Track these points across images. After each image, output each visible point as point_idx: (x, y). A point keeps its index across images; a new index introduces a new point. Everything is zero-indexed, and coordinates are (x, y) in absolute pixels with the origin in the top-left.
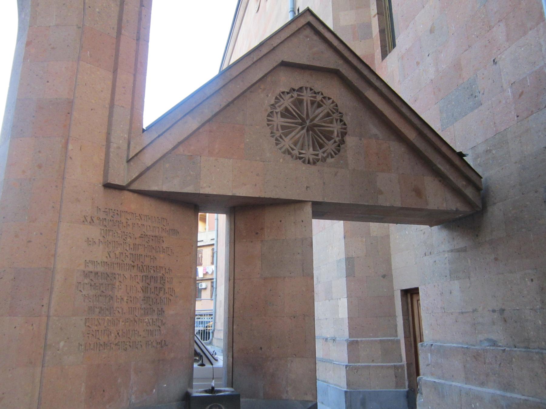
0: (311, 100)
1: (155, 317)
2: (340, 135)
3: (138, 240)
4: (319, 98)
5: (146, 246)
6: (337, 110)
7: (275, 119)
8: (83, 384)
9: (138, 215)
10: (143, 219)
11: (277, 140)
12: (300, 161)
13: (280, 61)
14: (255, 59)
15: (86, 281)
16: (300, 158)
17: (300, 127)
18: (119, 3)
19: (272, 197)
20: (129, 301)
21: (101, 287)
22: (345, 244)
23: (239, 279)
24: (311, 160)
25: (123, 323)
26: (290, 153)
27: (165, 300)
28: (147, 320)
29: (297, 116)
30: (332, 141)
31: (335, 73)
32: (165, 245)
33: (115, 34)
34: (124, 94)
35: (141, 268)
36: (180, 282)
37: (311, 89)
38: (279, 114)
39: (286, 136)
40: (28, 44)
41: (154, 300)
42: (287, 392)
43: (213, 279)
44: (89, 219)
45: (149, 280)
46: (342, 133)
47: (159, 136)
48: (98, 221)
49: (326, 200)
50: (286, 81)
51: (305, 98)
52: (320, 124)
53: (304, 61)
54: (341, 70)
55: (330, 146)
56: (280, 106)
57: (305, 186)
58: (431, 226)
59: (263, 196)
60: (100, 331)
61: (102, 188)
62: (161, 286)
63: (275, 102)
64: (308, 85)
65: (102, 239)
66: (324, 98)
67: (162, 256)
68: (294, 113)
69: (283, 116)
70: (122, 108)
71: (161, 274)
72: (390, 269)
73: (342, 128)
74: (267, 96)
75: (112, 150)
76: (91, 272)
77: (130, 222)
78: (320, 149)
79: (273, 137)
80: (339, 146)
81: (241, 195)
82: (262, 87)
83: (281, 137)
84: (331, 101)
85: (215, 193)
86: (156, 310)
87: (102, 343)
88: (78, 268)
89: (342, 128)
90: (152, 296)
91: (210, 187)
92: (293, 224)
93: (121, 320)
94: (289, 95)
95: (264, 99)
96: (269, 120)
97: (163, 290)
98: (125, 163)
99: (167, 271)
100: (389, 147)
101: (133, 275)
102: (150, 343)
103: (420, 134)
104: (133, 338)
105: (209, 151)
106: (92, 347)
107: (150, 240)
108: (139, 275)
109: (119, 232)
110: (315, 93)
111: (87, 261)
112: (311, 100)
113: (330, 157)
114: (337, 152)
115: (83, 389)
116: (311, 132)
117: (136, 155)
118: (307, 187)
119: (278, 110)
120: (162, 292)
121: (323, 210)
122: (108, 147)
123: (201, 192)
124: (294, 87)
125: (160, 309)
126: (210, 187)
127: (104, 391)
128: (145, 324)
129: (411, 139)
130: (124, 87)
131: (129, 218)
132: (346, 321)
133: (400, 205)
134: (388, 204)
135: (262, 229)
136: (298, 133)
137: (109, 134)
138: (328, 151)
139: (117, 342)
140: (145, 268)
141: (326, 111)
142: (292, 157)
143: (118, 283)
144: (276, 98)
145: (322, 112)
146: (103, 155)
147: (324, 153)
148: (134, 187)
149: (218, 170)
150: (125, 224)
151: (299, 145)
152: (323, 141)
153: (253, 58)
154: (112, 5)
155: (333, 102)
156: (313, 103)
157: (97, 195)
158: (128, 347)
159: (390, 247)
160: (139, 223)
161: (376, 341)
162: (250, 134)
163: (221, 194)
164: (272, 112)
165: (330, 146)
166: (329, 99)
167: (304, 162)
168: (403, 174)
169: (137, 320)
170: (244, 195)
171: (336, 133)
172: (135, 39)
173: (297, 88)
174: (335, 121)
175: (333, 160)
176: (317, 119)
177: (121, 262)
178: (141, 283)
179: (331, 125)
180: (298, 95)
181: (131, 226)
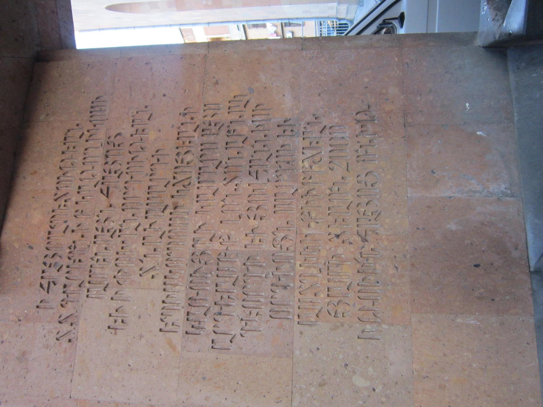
1: (299, 142)
5: (128, 178)
8: (459, 320)
9: (57, 204)
10: (63, 190)
15: (209, 325)
20: (260, 213)
25: (313, 224)
27: (256, 118)
28: (306, 164)
32: (127, 130)
35: (179, 187)
41: (258, 146)
44: (65, 328)
45: (210, 163)
62: (223, 132)
65: (110, 292)
67: (151, 135)
76: (188, 313)
86: (281, 141)
87: (359, 278)
88: (179, 348)
90: (247, 153)
93: (306, 231)
99: (188, 119)
101: (196, 206)
102: (361, 152)
104: (350, 198)
106: (368, 304)
107: (114, 168)
108: (196, 192)
111: (162, 325)
115: (472, 321)
120: (238, 128)
125: (280, 131)
127: (477, 266)
128: (315, 168)
131: (64, 226)
139: (358, 239)
140: (179, 177)
143: (216, 245)
150: (76, 236)
157: (11, 311)
160: (74, 199)
169: (307, 188)
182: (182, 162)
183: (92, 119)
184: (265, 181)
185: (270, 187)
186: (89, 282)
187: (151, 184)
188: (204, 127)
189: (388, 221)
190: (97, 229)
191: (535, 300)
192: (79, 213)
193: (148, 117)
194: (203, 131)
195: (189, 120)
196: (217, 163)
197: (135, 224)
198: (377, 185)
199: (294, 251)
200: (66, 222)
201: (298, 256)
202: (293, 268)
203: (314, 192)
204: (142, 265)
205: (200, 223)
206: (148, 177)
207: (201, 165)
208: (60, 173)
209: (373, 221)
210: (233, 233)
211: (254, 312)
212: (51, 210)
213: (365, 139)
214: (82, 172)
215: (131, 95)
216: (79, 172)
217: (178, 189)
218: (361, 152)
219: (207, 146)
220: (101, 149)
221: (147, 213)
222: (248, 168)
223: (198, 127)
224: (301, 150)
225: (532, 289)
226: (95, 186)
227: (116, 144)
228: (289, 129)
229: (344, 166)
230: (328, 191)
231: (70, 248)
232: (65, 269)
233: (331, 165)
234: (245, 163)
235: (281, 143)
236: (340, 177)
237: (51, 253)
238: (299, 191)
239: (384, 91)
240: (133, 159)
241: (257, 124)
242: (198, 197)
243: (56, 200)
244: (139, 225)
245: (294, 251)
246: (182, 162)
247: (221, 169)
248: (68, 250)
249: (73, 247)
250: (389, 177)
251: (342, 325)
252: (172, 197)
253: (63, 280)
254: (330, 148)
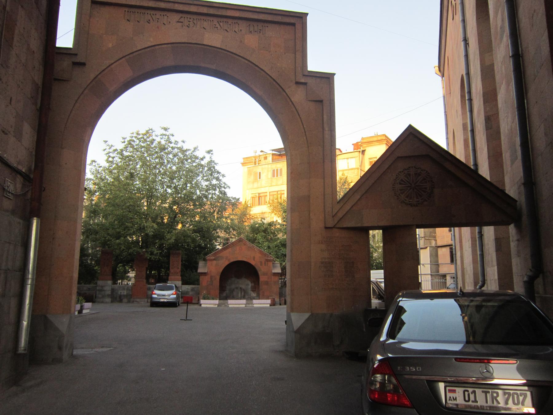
31: (427, 156)
40: (291, 173)
43: (452, 245)
69: (400, 184)
137: (324, 206)
148: (337, 226)
156: (416, 174)
167: (411, 206)
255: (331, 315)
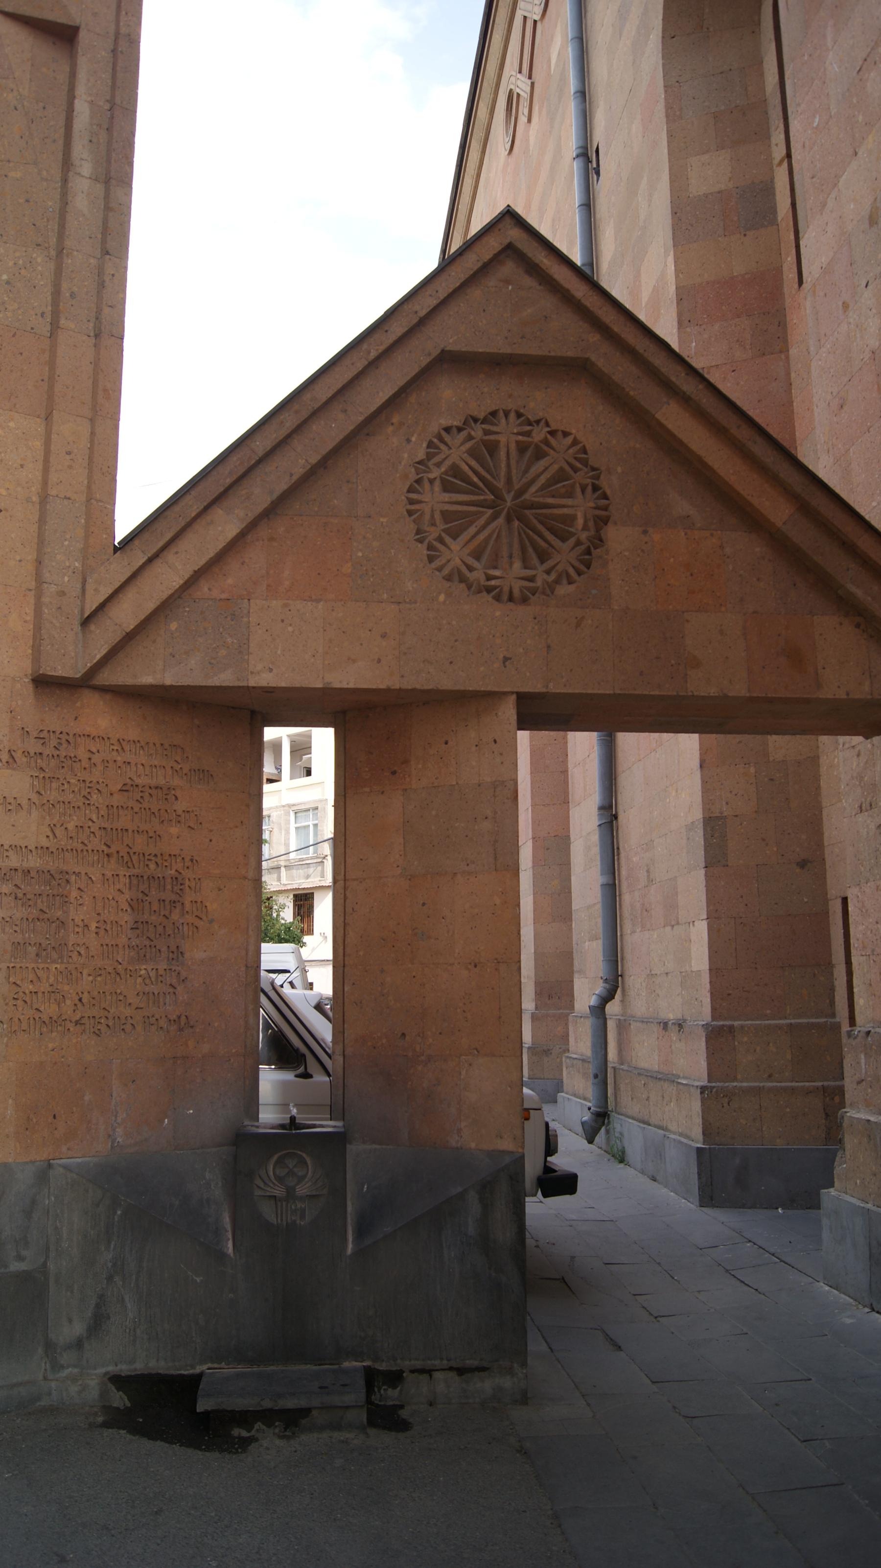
0: (517, 442)
2: (591, 524)
3: (116, 796)
4: (539, 434)
5: (136, 809)
6: (585, 462)
7: (426, 497)
8: (10, 1101)
10: (127, 748)
11: (430, 547)
12: (488, 598)
13: (435, 353)
14: (373, 354)
16: (489, 590)
17: (490, 512)
18: (53, 253)
19: (418, 687)
20: (102, 932)
21: (39, 901)
22: (704, 782)
23: (356, 880)
24: (516, 593)
25: (91, 978)
26: (462, 579)
28: (143, 972)
29: (481, 485)
30: (572, 541)
31: (577, 369)
33: (49, 328)
34: (70, 467)
35: (126, 858)
36: (220, 890)
37: (519, 415)
38: (437, 483)
39: (455, 537)
41: (160, 929)
42: (459, 1131)
46: (597, 518)
47: (150, 560)
48: (25, 760)
49: (553, 688)
50: (453, 399)
51: (503, 439)
52: (541, 500)
53: (499, 346)
54: (593, 358)
55: (565, 555)
56: (438, 465)
57: (501, 657)
58: (867, 738)
59: (397, 687)
60: (40, 995)
61: (31, 687)
62: (174, 897)
63: (427, 454)
64: (511, 405)
65: (35, 797)
66: (552, 433)
67: (174, 830)
68: (475, 479)
69: (447, 487)
70: (66, 502)
71: (173, 872)
72: (820, 845)
73: (597, 508)
74: (408, 441)
75: (46, 600)
76: (16, 870)
77: (96, 758)
78: (542, 562)
79: (420, 541)
80: (588, 552)
81: (344, 685)
82: (395, 420)
83: (440, 540)
84: (569, 440)
85: (283, 685)
86: (164, 949)
87: (45, 1018)
89: (597, 508)
90: (154, 918)
91: (271, 670)
92: (474, 749)
93: (85, 972)
94: (464, 434)
95: (399, 449)
96: (411, 502)
97: (178, 905)
98: (77, 628)
100: (721, 547)
101: (109, 874)
103: (804, 508)
104: (112, 1010)
105: (268, 586)
107: (146, 795)
108: (121, 873)
109: (73, 781)
110: (530, 424)
112: (517, 442)
113: (565, 581)
114: (582, 568)
116: (516, 523)
117: (102, 606)
118: (506, 659)
119: (435, 473)
120: (177, 911)
121: (543, 713)
122: (39, 595)
123: (252, 683)
124: (475, 413)
125: (173, 948)
126: (271, 670)
127: (54, 1117)
128: (139, 980)
129: (779, 524)
130: (68, 453)
131: (94, 750)
132: (706, 978)
133: (744, 693)
134: (713, 691)
135: (406, 762)
136: (484, 527)
138: (560, 568)
139: (78, 1017)
140: (135, 858)
141: (556, 467)
142: (469, 587)
143: (74, 893)
144: (430, 445)
145: (546, 469)
146: (29, 610)
147: (548, 572)
149: (290, 629)
150: (85, 763)
151: (485, 558)
152: (546, 541)
153: (369, 352)
154: (39, 260)
155: (575, 442)
156: (522, 448)
157: (20, 702)
158: (103, 1028)
159: (818, 788)
160: (119, 758)
161: (779, 1027)
162: (364, 538)
163: (298, 685)
164: (418, 481)
165: (565, 555)
166: (566, 434)
167: (498, 598)
168: (755, 612)
169: (122, 973)
170: (351, 686)
171: (580, 521)
172: (92, 334)
173: (481, 416)
174: (578, 490)
175: (572, 588)
176: (533, 489)
177: (80, 847)
178: (126, 891)
179: (569, 502)
180: (487, 432)
181: (100, 767)
182: (149, 860)
183: (193, 772)
184: (129, 936)
185: (123, 940)
186: (44, 777)
187: (130, 831)
188: (180, 879)
189: (93, 1042)
190: (91, 782)
191: (27, 1163)
192: (106, 764)
193: (192, 825)
194: (176, 878)
195: (186, 864)
196: (146, 892)
197: (94, 818)
198: (122, 1033)
199: (68, 963)
200: (98, 752)
201: (64, 966)
202: (54, 962)
203: (118, 979)
204: (58, 826)
205: (93, 878)
206: (136, 828)
207: (145, 878)
208: (143, 744)
209: (92, 1030)
210: (85, 908)
211: (17, 929)
212: (110, 736)
213: (163, 1023)
214: (143, 765)
215: (213, 808)
216: (143, 762)
217: (125, 858)
218: (153, 1020)
219: (162, 883)
220: (164, 782)
221: (104, 828)
222: (141, 920)
223: (180, 873)
224: (155, 967)
225: (35, 1161)
226: (130, 778)
227: (168, 797)
228: (175, 956)
229: (141, 1005)
230: (119, 991)
231: (75, 757)
232: (56, 753)
233: (141, 994)
234: (146, 917)
235: (162, 950)
236: (131, 1001)
237: (71, 738)
238: (120, 966)
239: (205, 1040)
240: (153, 813)
241: (181, 927)
242: (117, 875)
243: (119, 740)
244: (93, 822)
245: (68, 963)
246: (149, 860)
247: (141, 896)
248: (73, 755)
249: (75, 759)
250: (130, 1043)
251: (7, 1004)
252: (118, 852)
253: (47, 752)
254: (156, 993)
255: (43, 1174)
